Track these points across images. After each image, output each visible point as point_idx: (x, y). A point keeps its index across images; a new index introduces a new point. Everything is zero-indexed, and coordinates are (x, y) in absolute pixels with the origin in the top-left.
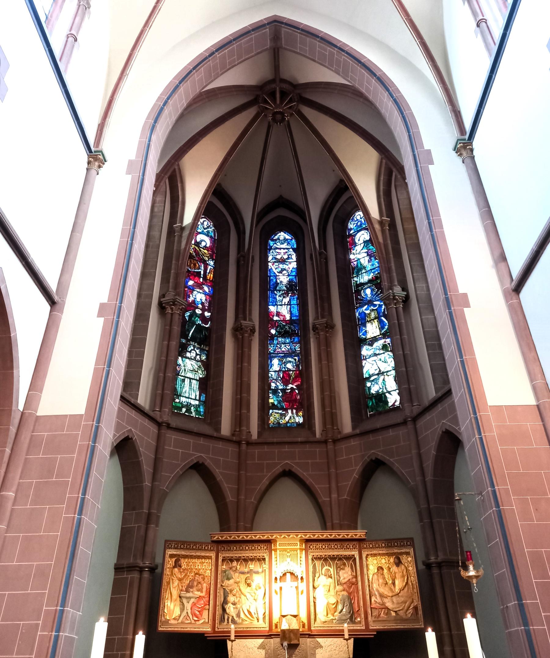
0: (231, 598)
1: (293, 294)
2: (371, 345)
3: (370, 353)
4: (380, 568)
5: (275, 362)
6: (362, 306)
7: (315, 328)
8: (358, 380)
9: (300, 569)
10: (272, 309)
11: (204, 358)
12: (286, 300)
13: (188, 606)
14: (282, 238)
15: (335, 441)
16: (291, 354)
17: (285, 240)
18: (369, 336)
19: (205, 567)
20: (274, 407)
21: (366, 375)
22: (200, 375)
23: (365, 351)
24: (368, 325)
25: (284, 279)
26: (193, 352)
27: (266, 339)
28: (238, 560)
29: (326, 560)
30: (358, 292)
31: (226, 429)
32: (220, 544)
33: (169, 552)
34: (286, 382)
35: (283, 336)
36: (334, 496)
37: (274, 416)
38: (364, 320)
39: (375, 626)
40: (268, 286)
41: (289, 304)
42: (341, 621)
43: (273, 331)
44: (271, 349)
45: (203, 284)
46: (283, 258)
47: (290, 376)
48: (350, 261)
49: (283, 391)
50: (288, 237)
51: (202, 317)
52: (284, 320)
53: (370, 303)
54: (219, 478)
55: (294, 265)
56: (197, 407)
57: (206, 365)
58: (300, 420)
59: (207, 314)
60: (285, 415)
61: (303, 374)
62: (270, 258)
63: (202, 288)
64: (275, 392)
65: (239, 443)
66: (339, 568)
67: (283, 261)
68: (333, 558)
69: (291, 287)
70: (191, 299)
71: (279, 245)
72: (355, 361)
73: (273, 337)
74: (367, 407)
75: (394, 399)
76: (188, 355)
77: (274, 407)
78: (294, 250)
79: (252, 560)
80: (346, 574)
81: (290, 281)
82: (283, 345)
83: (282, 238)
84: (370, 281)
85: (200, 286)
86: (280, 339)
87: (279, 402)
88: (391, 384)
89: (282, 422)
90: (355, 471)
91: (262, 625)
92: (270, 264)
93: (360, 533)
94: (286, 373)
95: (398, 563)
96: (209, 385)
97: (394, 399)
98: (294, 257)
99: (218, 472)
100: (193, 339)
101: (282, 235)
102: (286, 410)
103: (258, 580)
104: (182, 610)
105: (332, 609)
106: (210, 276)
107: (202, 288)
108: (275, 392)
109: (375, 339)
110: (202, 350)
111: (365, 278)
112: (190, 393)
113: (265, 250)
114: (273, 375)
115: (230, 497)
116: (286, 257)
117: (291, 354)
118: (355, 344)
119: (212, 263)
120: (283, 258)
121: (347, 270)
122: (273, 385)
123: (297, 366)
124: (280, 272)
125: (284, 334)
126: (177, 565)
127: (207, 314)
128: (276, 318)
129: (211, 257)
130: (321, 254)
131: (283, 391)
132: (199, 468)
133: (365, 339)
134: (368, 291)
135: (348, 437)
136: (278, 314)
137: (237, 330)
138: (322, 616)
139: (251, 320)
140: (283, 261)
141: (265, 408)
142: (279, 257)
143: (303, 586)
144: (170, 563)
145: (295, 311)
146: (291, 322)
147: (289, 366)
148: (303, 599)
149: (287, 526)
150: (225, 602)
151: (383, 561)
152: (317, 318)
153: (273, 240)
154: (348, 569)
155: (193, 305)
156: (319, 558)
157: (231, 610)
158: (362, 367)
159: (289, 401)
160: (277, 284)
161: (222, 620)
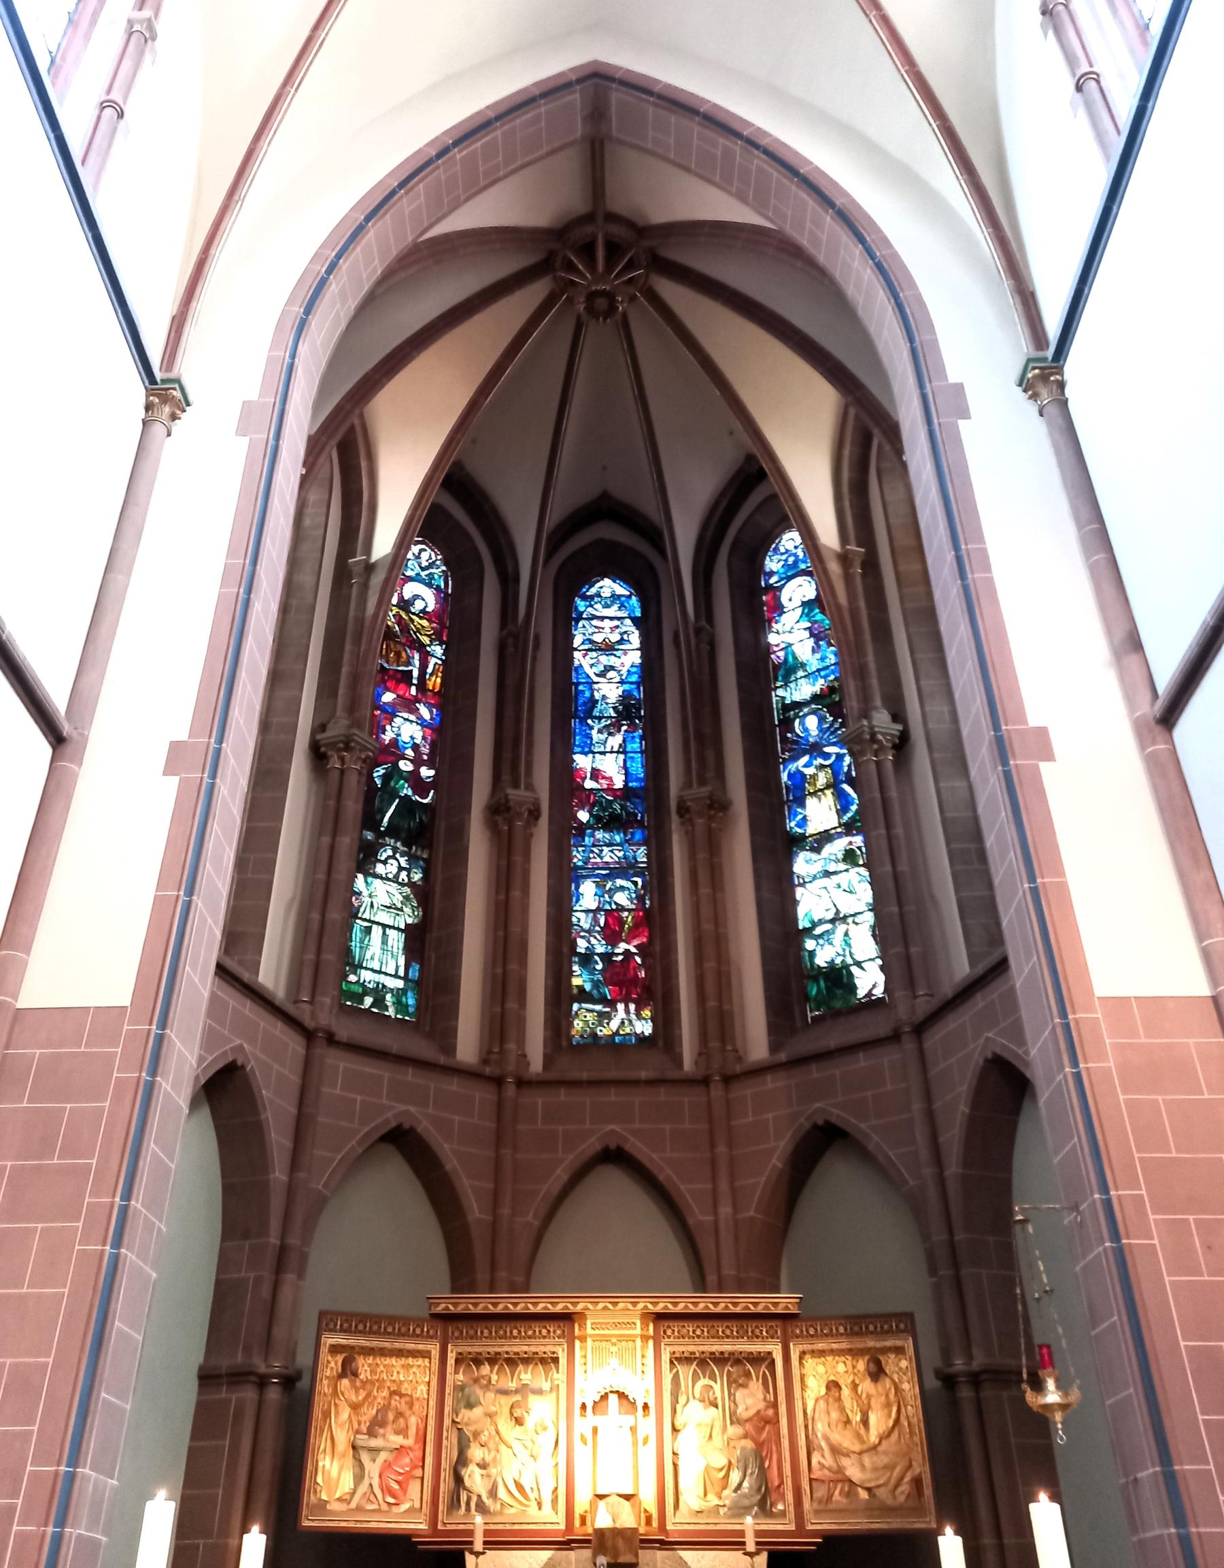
0: (476, 1453)
1: (633, 728)
2: (817, 850)
3: (817, 868)
4: (833, 1386)
5: (588, 889)
6: (795, 758)
7: (683, 810)
8: (784, 934)
9: (641, 1387)
10: (582, 762)
11: (417, 877)
12: (615, 741)
13: (373, 1469)
14: (606, 593)
15: (728, 1080)
16: (625, 869)
17: (615, 597)
18: (812, 828)
19: (413, 1376)
20: (583, 996)
21: (803, 923)
22: (408, 917)
23: (803, 864)
24: (811, 802)
25: (610, 692)
26: (391, 862)
27: (566, 834)
28: (493, 1360)
29: (703, 1362)
30: (787, 724)
31: (468, 1044)
32: (449, 1323)
33: (329, 1340)
34: (612, 934)
35: (607, 827)
36: (725, 1210)
37: (583, 1019)
38: (800, 790)
39: (819, 1524)
40: (571, 706)
41: (623, 750)
42: (739, 1510)
43: (583, 816)
44: (578, 857)
45: (417, 700)
46: (608, 641)
47: (621, 922)
48: (768, 649)
49: (607, 957)
50: (621, 590)
51: (414, 779)
52: (610, 790)
53: (815, 749)
54: (451, 1163)
55: (635, 657)
56: (399, 994)
57: (422, 895)
58: (645, 1028)
59: (426, 772)
60: (608, 1017)
61: (653, 918)
62: (577, 641)
63: (415, 711)
64: (586, 960)
65: (499, 1082)
66: (734, 1383)
67: (608, 648)
68: (721, 1359)
69: (626, 711)
70: (388, 737)
71: (600, 610)
72: (778, 889)
73: (582, 829)
74: (806, 998)
75: (870, 980)
76: (380, 869)
77: (583, 996)
78: (635, 620)
79: (527, 1360)
80: (751, 1399)
81: (626, 696)
82: (608, 849)
83: (606, 593)
84: (815, 698)
85: (409, 705)
86: (599, 835)
87: (596, 984)
88: (864, 945)
89: (603, 1032)
90: (777, 1151)
91: (551, 1519)
92: (577, 655)
93: (785, 1301)
94: (613, 914)
95: (877, 1373)
96: (428, 942)
97: (870, 980)
98: (635, 639)
99: (447, 1151)
100: (393, 831)
101: (607, 586)
102: (612, 1004)
103: (541, 1409)
104: (359, 1477)
105: (715, 1482)
106: (435, 682)
107: (415, 711)
109: (826, 837)
110: (412, 859)
111: (802, 690)
112: (382, 960)
113: (566, 620)
115: (476, 1211)
116: (615, 637)
117: (625, 869)
118: (779, 847)
119: (438, 650)
120: (608, 641)
121: (762, 670)
122: (582, 945)
123: (640, 899)
124: (602, 674)
125: (610, 822)
126: (348, 1370)
127: (426, 772)
128: (589, 784)
129: (437, 637)
130: (698, 631)
131: (607, 957)
132: (402, 1140)
133: (803, 837)
134: (812, 722)
135: (760, 1070)
136: (596, 774)
137: (498, 810)
138: (692, 1497)
139: (530, 787)
140: (608, 648)
141: (561, 998)
142: (598, 638)
143: (647, 1425)
144: (331, 1365)
145: (637, 768)
146: (626, 793)
147: (622, 899)
148: (648, 1455)
149: (611, 1283)
150: (462, 1460)
151: (841, 1368)
152: (688, 784)
153: (584, 597)
154: (756, 1386)
155: (393, 751)
156: (687, 1360)
157: (474, 1479)
158: (795, 903)
159: (621, 983)
160: (593, 702)
161: (454, 1503)
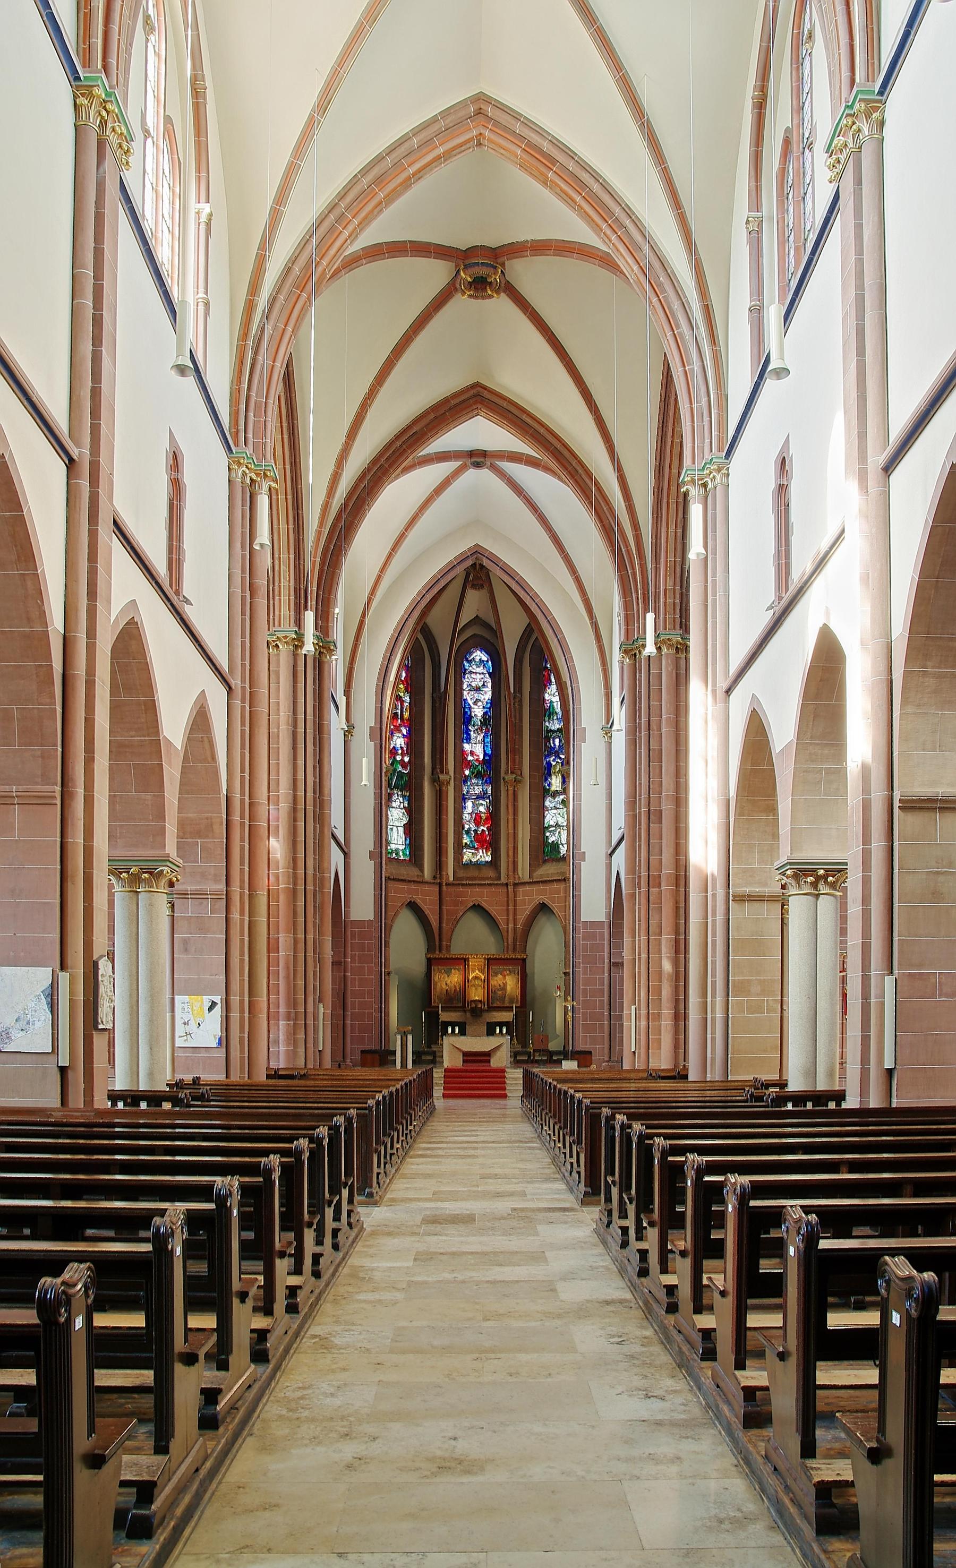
5: (469, 804)
10: (467, 747)
14: (477, 659)
17: (481, 661)
30: (548, 739)
37: (468, 855)
46: (477, 688)
47: (481, 818)
49: (475, 831)
52: (477, 760)
62: (465, 686)
63: (400, 731)
67: (478, 689)
69: (485, 720)
72: (539, 811)
78: (490, 674)
83: (477, 659)
87: (471, 841)
92: (465, 693)
94: (478, 815)
102: (477, 849)
106: (406, 715)
107: (400, 731)
108: (468, 832)
114: (466, 816)
119: (407, 699)
120: (477, 688)
122: (467, 827)
123: (488, 808)
125: (478, 775)
128: (470, 758)
131: (475, 831)
136: (472, 753)
141: (459, 847)
145: (489, 751)
147: (482, 809)
158: (544, 817)
159: (481, 841)
